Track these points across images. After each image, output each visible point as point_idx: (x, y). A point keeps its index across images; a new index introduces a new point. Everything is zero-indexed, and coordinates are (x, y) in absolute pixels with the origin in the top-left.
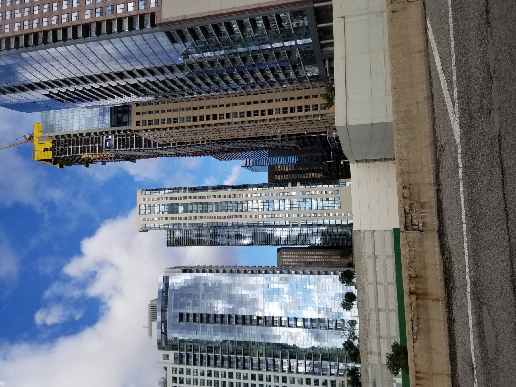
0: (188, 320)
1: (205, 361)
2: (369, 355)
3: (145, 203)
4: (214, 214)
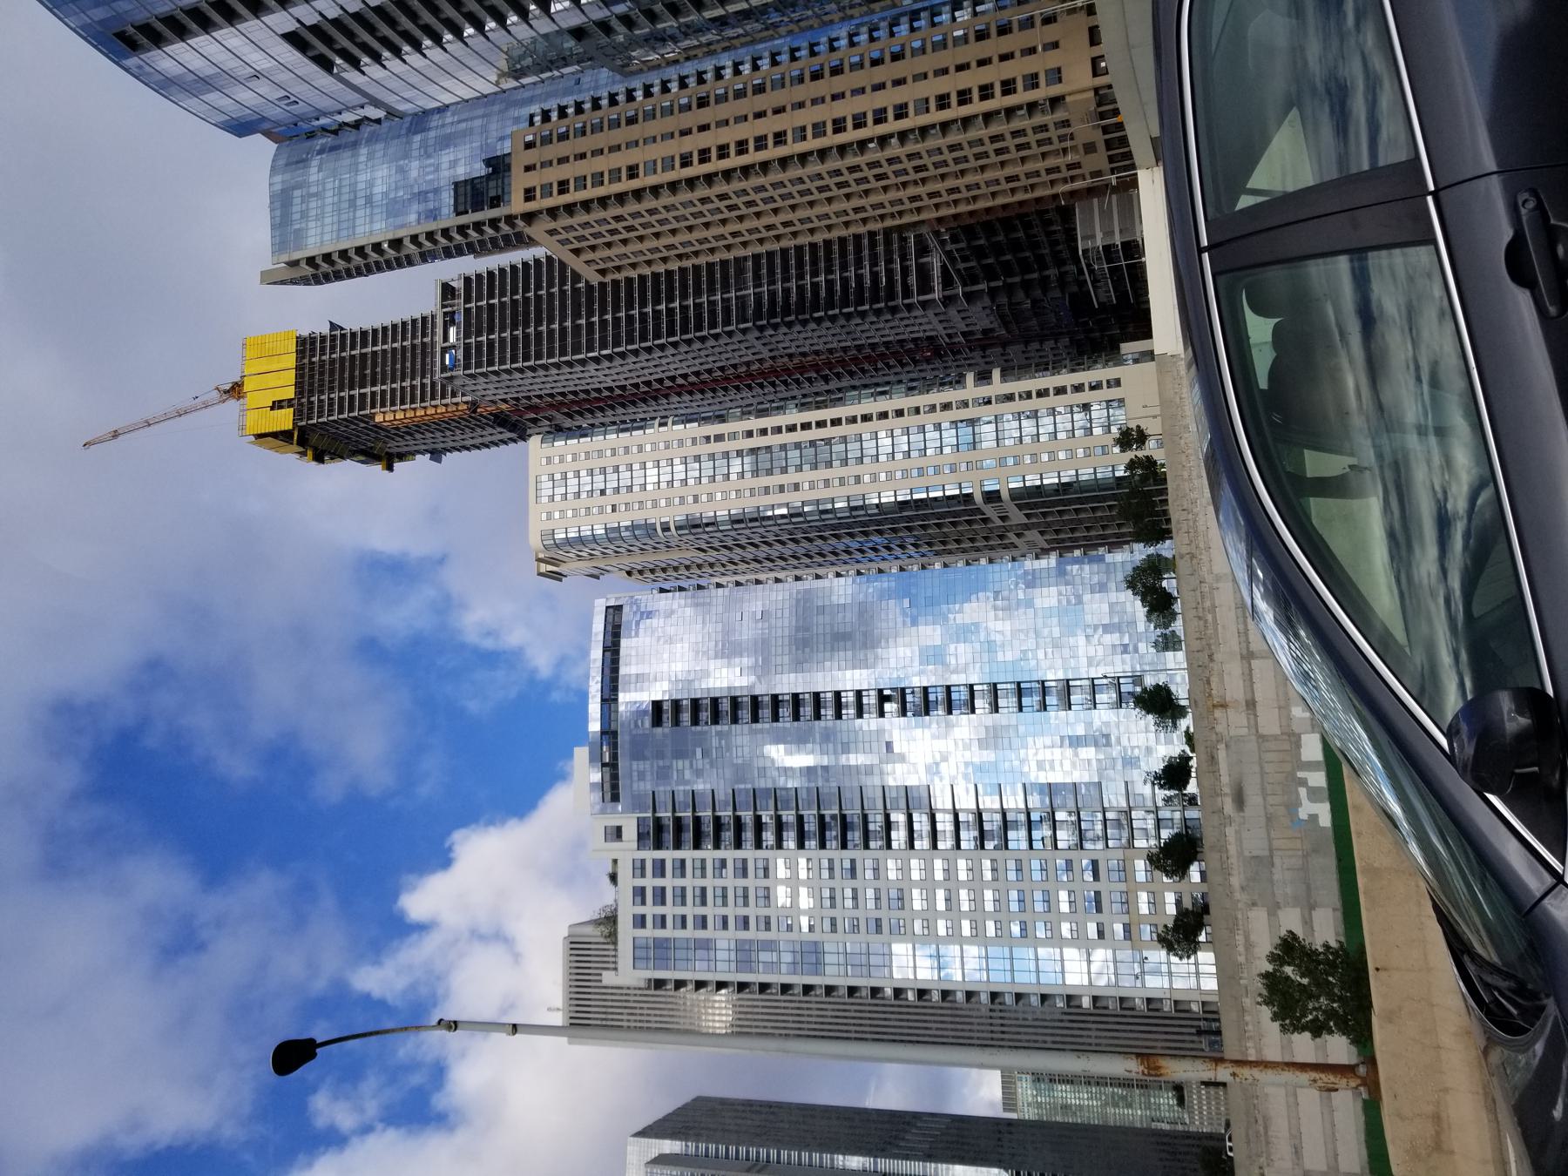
0: (676, 722)
1: (728, 835)
2: (1218, 713)
3: (550, 469)
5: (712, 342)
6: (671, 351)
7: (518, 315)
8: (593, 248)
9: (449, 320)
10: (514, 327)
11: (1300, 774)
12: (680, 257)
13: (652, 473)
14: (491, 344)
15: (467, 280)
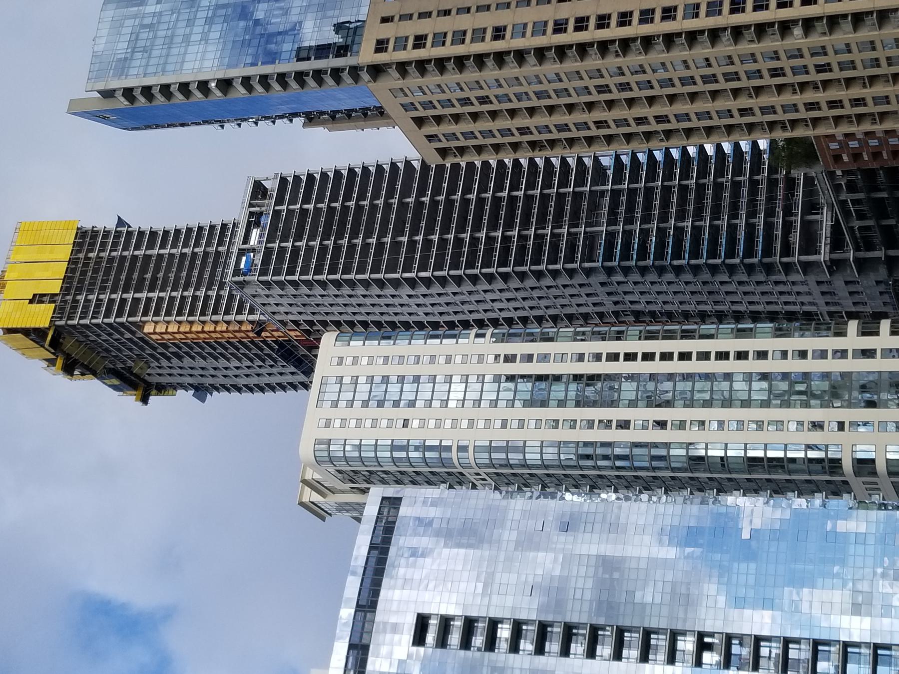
4: (572, 412)
5: (548, 281)
6: (500, 284)
7: (334, 224)
8: (439, 119)
9: (254, 220)
10: (326, 236)
12: (533, 145)
13: (458, 389)
14: (296, 251)
15: (283, 181)
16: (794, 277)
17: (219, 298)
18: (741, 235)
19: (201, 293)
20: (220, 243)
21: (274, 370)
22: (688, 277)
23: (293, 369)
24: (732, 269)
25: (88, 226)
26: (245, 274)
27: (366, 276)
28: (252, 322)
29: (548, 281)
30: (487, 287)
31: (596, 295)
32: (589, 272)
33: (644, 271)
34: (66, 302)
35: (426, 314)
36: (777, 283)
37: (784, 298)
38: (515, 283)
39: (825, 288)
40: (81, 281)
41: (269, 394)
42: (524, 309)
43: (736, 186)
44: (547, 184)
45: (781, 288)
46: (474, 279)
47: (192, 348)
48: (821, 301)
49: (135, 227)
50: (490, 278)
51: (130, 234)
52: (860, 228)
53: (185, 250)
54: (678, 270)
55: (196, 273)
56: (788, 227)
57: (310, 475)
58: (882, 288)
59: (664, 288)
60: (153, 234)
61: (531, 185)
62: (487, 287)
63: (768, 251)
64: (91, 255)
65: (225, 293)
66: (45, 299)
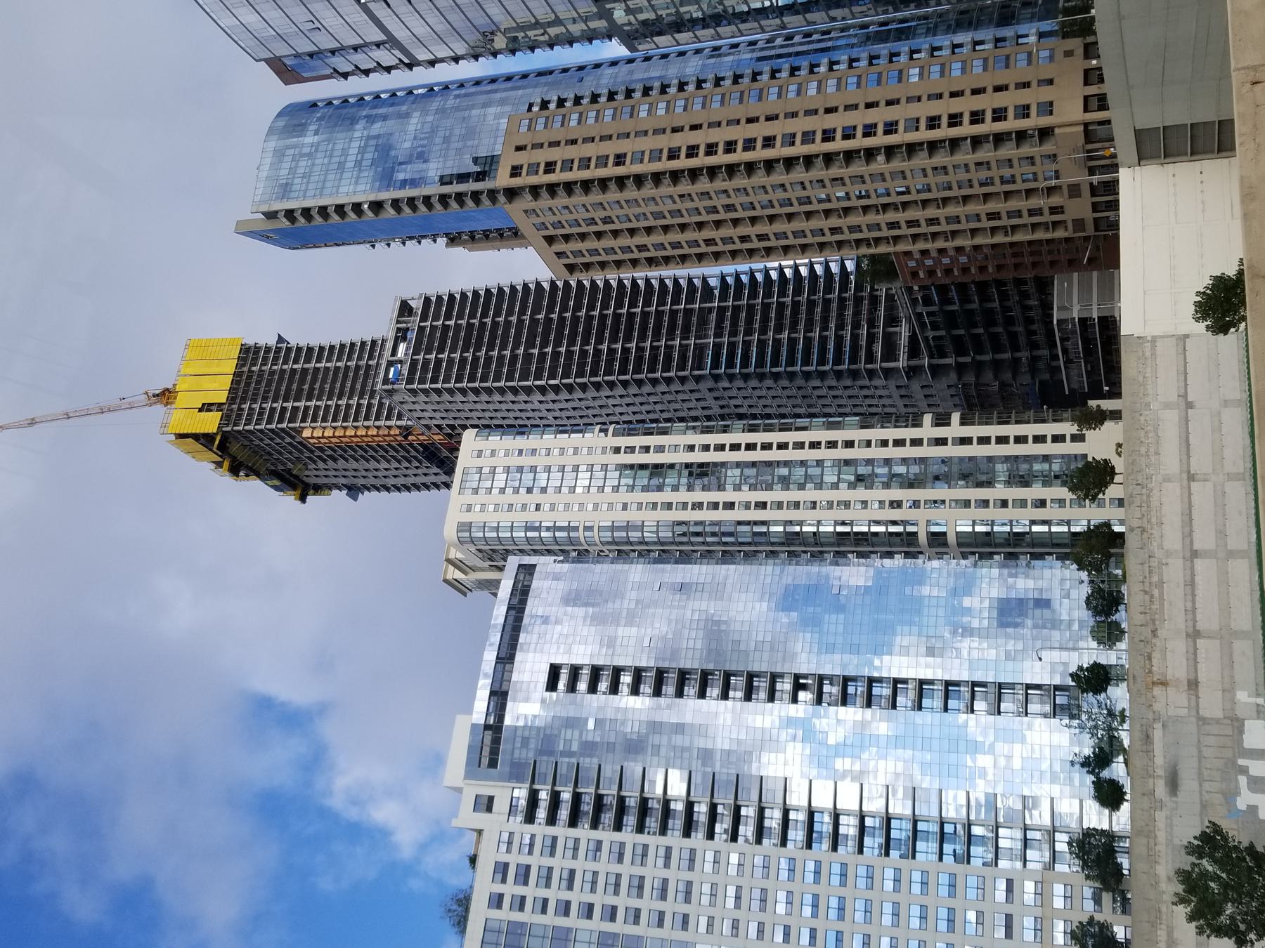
2: (1157, 691)
5: (663, 387)
6: (620, 390)
7: (472, 338)
9: (401, 335)
10: (465, 349)
11: (1241, 762)
14: (438, 362)
15: (427, 300)
16: (877, 382)
17: (370, 405)
18: (831, 346)
19: (354, 402)
20: (371, 357)
21: (419, 471)
22: (785, 383)
23: (436, 470)
24: (822, 375)
25: (250, 342)
26: (393, 383)
27: (501, 384)
28: (399, 427)
29: (663, 387)
30: (609, 393)
31: (705, 399)
32: (698, 379)
33: (746, 377)
34: (232, 410)
35: (555, 418)
36: (861, 388)
37: (868, 401)
38: (633, 389)
39: (903, 392)
40: (245, 392)
41: (415, 493)
42: (641, 413)
43: (827, 303)
44: (662, 302)
45: (865, 392)
46: (598, 386)
47: (345, 451)
48: (900, 403)
49: (293, 343)
50: (611, 385)
51: (289, 349)
52: (934, 338)
53: (339, 364)
54: (776, 376)
55: (348, 384)
56: (871, 338)
57: (455, 554)
58: (953, 391)
59: (764, 393)
60: (310, 350)
61: (647, 303)
62: (609, 393)
63: (854, 359)
64: (254, 369)
65: (376, 402)
66: (215, 407)
